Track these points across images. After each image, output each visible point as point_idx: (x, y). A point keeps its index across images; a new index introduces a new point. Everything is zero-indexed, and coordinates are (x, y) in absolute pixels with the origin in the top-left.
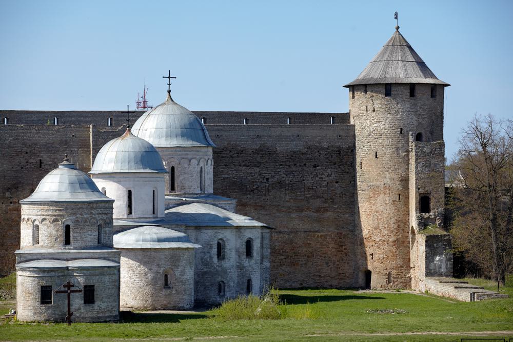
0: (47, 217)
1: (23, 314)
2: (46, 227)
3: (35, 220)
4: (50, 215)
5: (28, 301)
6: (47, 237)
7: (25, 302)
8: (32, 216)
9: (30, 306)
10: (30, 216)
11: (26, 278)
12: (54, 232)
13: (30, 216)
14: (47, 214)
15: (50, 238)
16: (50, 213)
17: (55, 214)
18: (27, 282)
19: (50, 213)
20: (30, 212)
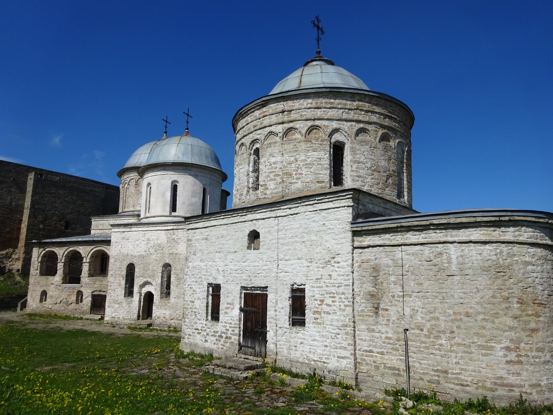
0: (370, 127)
1: (512, 379)
2: (367, 147)
3: (336, 130)
4: (375, 123)
5: (534, 330)
6: (370, 171)
7: (523, 334)
8: (326, 123)
9: (539, 350)
10: (317, 123)
11: (516, 249)
12: (383, 163)
13: (317, 123)
14: (367, 119)
15: (376, 174)
16: (374, 118)
17: (383, 123)
18: (527, 263)
19: (374, 118)
20: (319, 113)
